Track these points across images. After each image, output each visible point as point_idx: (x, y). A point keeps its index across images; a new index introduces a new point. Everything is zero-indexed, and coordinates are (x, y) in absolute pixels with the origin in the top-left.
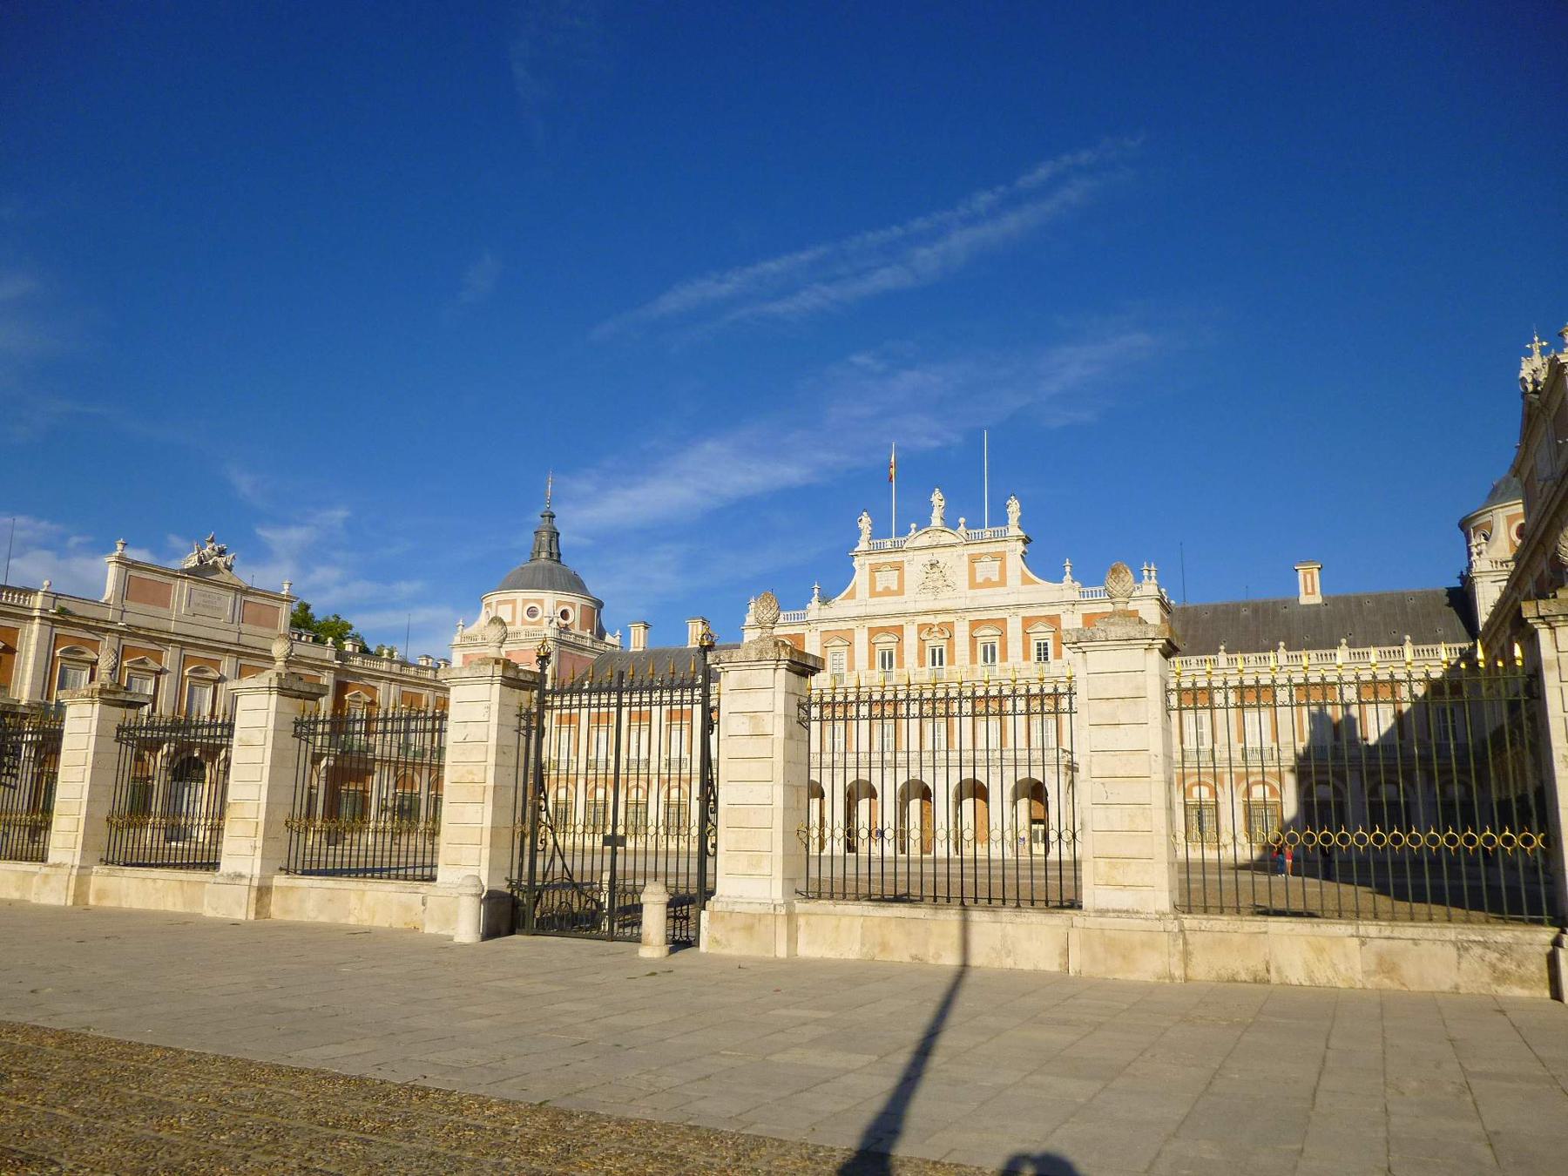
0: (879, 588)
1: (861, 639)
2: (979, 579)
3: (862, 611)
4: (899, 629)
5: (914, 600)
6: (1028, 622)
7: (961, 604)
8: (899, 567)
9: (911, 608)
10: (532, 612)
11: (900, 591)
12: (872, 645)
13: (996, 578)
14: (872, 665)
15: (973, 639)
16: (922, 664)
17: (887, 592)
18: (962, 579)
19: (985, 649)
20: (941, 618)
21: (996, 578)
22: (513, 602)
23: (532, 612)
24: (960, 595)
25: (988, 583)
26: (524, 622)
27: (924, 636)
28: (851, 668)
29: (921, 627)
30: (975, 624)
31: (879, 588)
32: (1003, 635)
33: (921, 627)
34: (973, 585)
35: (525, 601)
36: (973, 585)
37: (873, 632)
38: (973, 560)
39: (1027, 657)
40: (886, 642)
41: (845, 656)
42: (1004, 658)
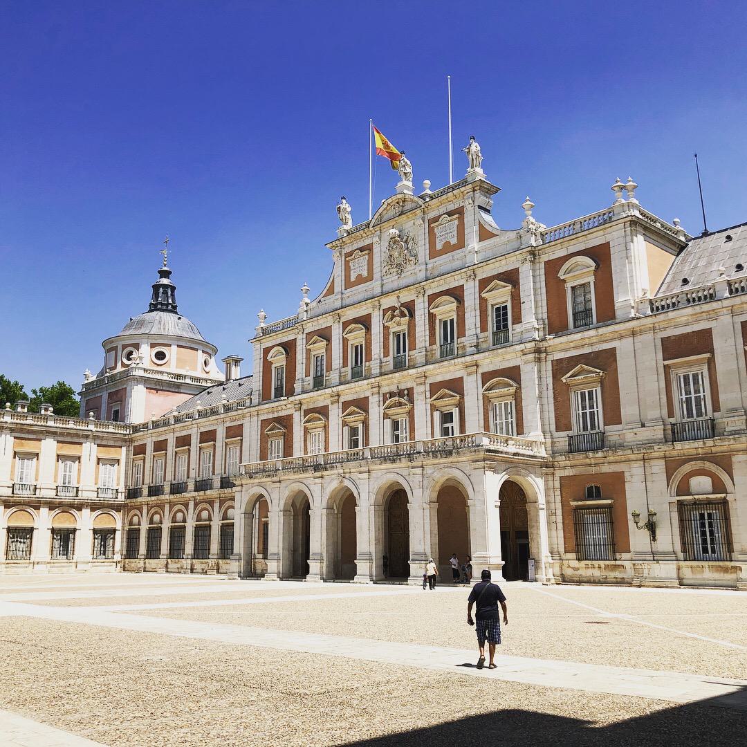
18: (422, 250)
28: (329, 368)
34: (434, 253)
36: (434, 253)
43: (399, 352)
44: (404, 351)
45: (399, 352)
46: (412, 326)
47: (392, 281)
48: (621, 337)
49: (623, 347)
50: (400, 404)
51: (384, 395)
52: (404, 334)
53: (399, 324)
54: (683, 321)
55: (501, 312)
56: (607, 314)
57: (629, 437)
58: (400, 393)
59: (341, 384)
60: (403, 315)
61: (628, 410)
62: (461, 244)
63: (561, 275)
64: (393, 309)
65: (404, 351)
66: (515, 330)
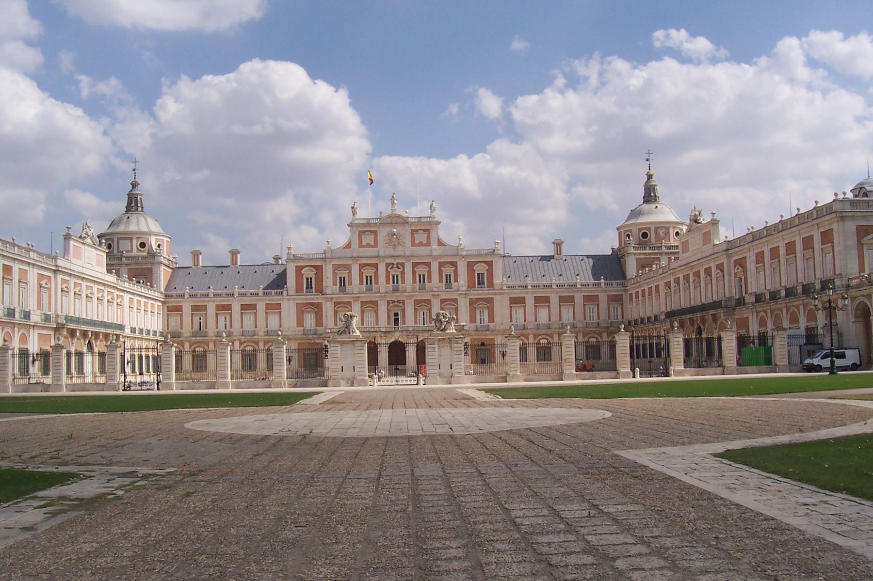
0: (364, 243)
1: (355, 269)
2: (417, 242)
3: (355, 255)
4: (376, 266)
5: (383, 249)
6: (441, 265)
7: (408, 253)
8: (375, 233)
9: (381, 254)
10: (143, 245)
11: (376, 246)
12: (361, 274)
13: (425, 242)
14: (361, 283)
15: (414, 273)
16: (388, 282)
17: (368, 245)
18: (408, 242)
19: (420, 276)
23: (143, 245)
24: (407, 248)
29: (387, 265)
30: (415, 265)
31: (364, 243)
32: (429, 272)
34: (413, 244)
37: (362, 266)
38: (414, 232)
39: (441, 281)
40: (369, 272)
42: (430, 281)
46: (403, 273)
47: (390, 251)
48: (496, 294)
49: (497, 299)
50: (397, 306)
54: (517, 293)
55: (448, 278)
56: (491, 285)
57: (497, 328)
58: (399, 302)
59: (360, 293)
60: (398, 268)
61: (497, 319)
62: (428, 244)
66: (454, 285)
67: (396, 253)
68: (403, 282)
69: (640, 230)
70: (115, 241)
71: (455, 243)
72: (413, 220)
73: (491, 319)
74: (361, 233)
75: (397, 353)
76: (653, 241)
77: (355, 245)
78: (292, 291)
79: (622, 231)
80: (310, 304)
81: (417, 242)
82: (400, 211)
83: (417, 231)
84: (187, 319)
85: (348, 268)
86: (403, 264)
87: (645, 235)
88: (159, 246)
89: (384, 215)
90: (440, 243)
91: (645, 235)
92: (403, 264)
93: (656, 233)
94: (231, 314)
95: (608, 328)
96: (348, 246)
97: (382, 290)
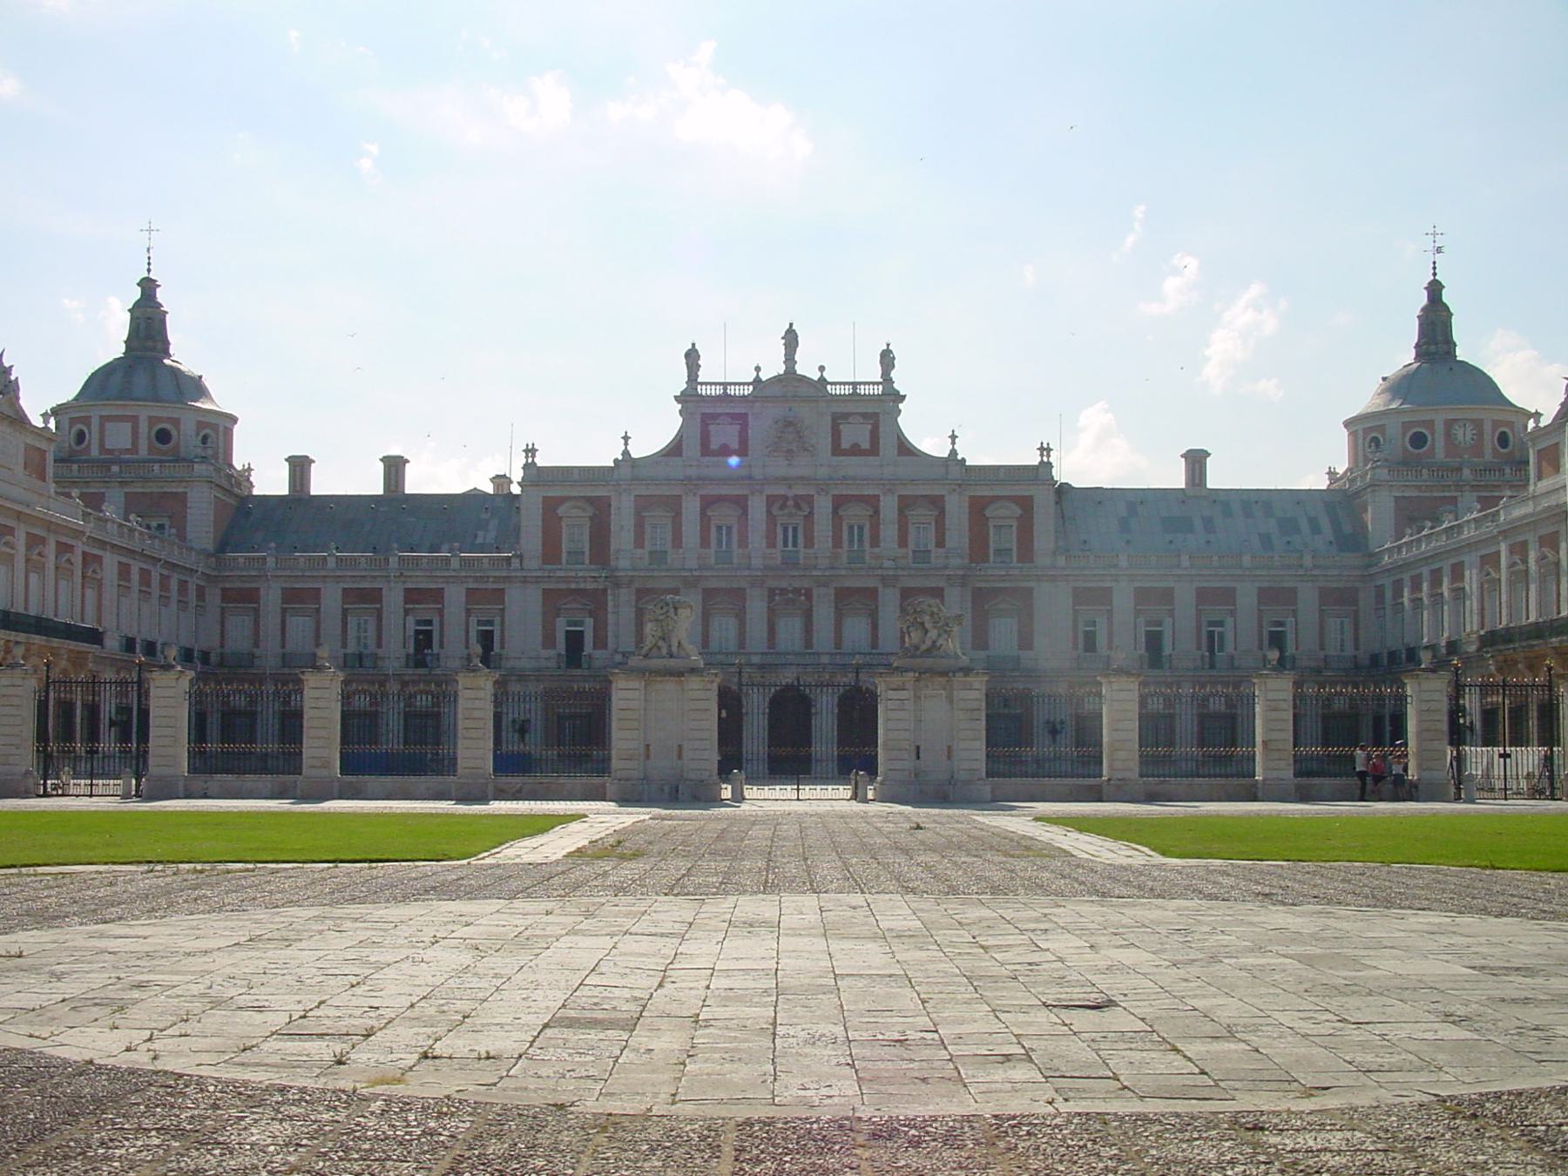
2: (845, 445)
3: (693, 472)
4: (741, 503)
7: (823, 472)
8: (742, 419)
10: (163, 436)
13: (866, 445)
16: (771, 544)
19: (851, 528)
20: (800, 490)
21: (866, 445)
22: (134, 420)
23: (163, 436)
25: (855, 451)
26: (151, 449)
27: (775, 511)
29: (771, 500)
33: (771, 500)
34: (837, 450)
35: (152, 420)
41: (669, 528)
43: (785, 544)
44: (795, 544)
45: (785, 544)
46: (809, 518)
47: (778, 467)
51: (772, 593)
52: (795, 530)
53: (790, 515)
58: (797, 591)
59: (700, 568)
60: (798, 506)
62: (874, 450)
63: (988, 513)
64: (786, 498)
65: (795, 544)
67: (792, 472)
68: (809, 542)
69: (1406, 426)
70: (95, 422)
71: (942, 451)
72: (839, 390)
73: (1026, 642)
74: (707, 420)
75: (791, 713)
76: (1440, 453)
77: (692, 449)
78: (533, 563)
79: (1360, 427)
80: (578, 591)
81: (845, 445)
82: (806, 367)
83: (846, 416)
84: (271, 622)
85: (674, 505)
86: (809, 499)
87: (1418, 440)
88: (205, 439)
89: (764, 376)
90: (905, 449)
91: (1418, 440)
92: (809, 499)
93: (1448, 435)
94: (379, 612)
95: (1319, 671)
96: (675, 449)
97: (757, 562)
